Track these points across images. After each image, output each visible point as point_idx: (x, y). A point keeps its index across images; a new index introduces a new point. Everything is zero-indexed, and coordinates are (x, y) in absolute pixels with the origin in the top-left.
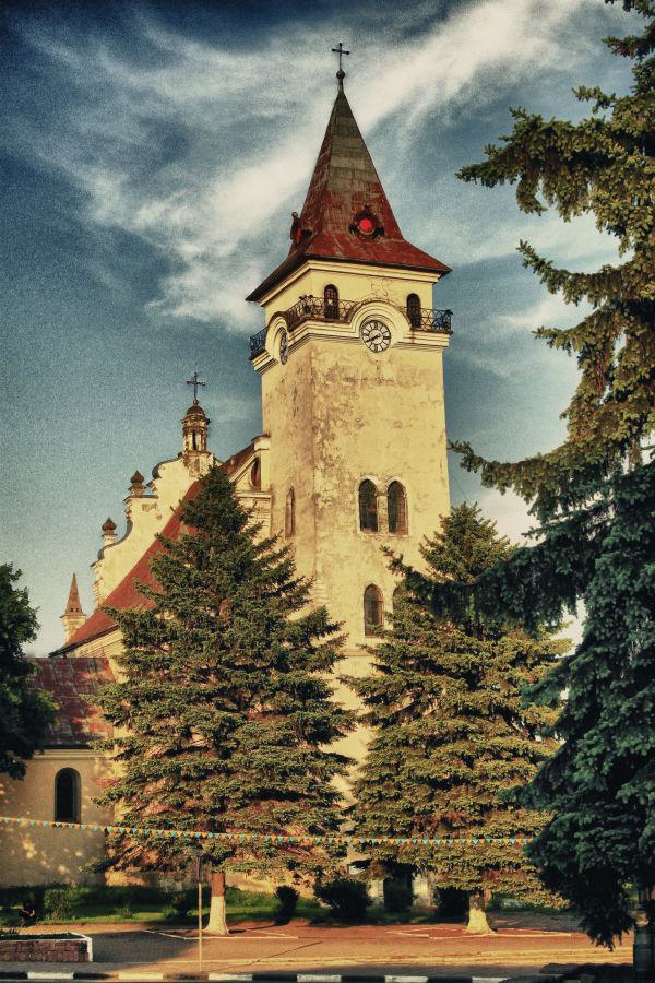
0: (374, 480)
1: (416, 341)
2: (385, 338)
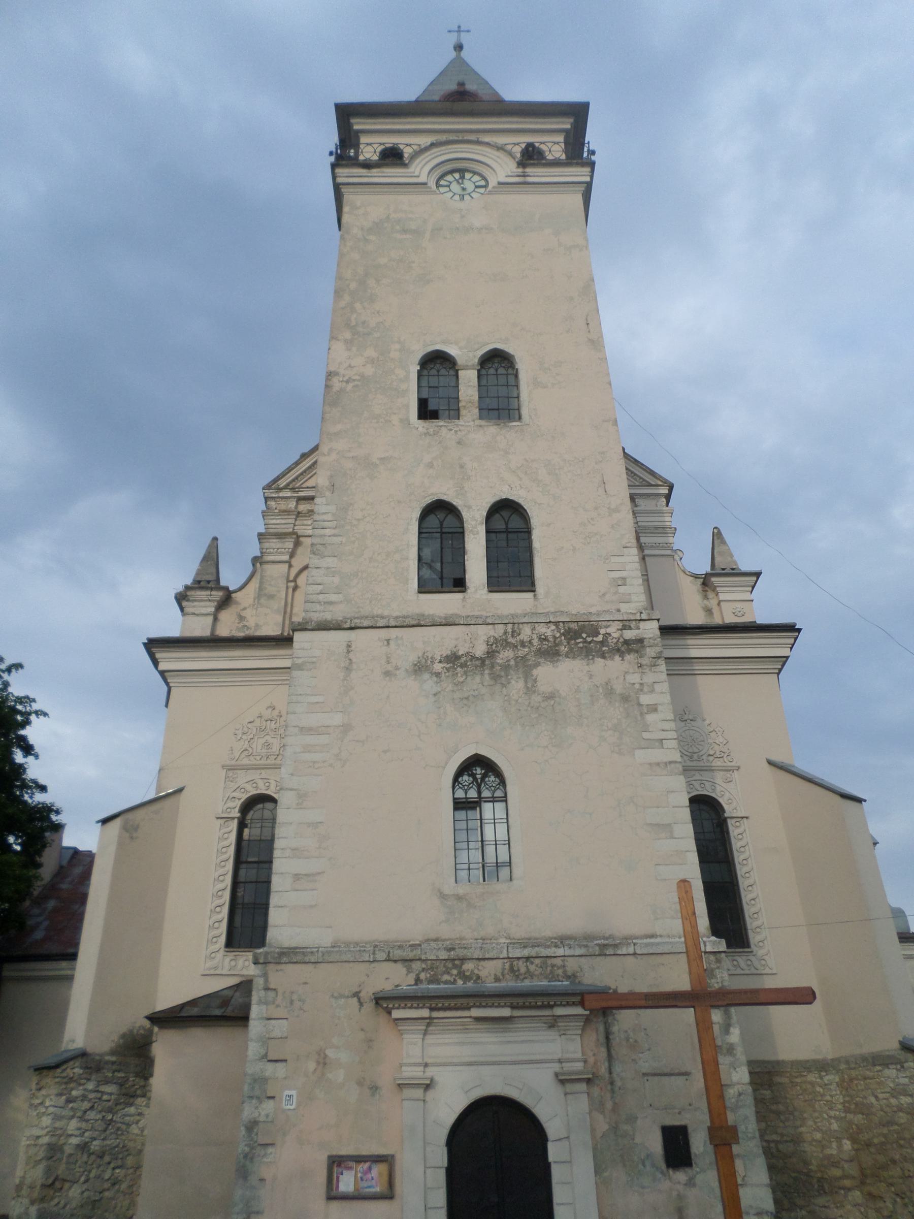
0: (452, 351)
1: (530, 179)
2: (477, 187)
